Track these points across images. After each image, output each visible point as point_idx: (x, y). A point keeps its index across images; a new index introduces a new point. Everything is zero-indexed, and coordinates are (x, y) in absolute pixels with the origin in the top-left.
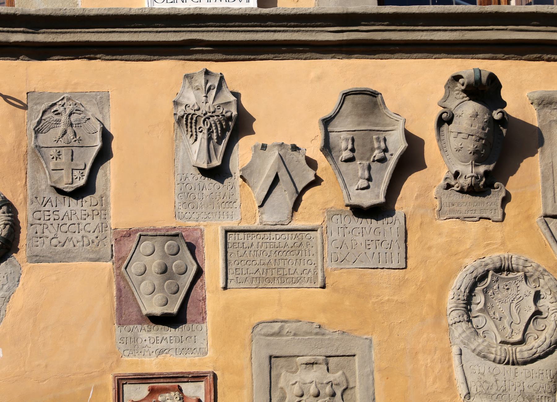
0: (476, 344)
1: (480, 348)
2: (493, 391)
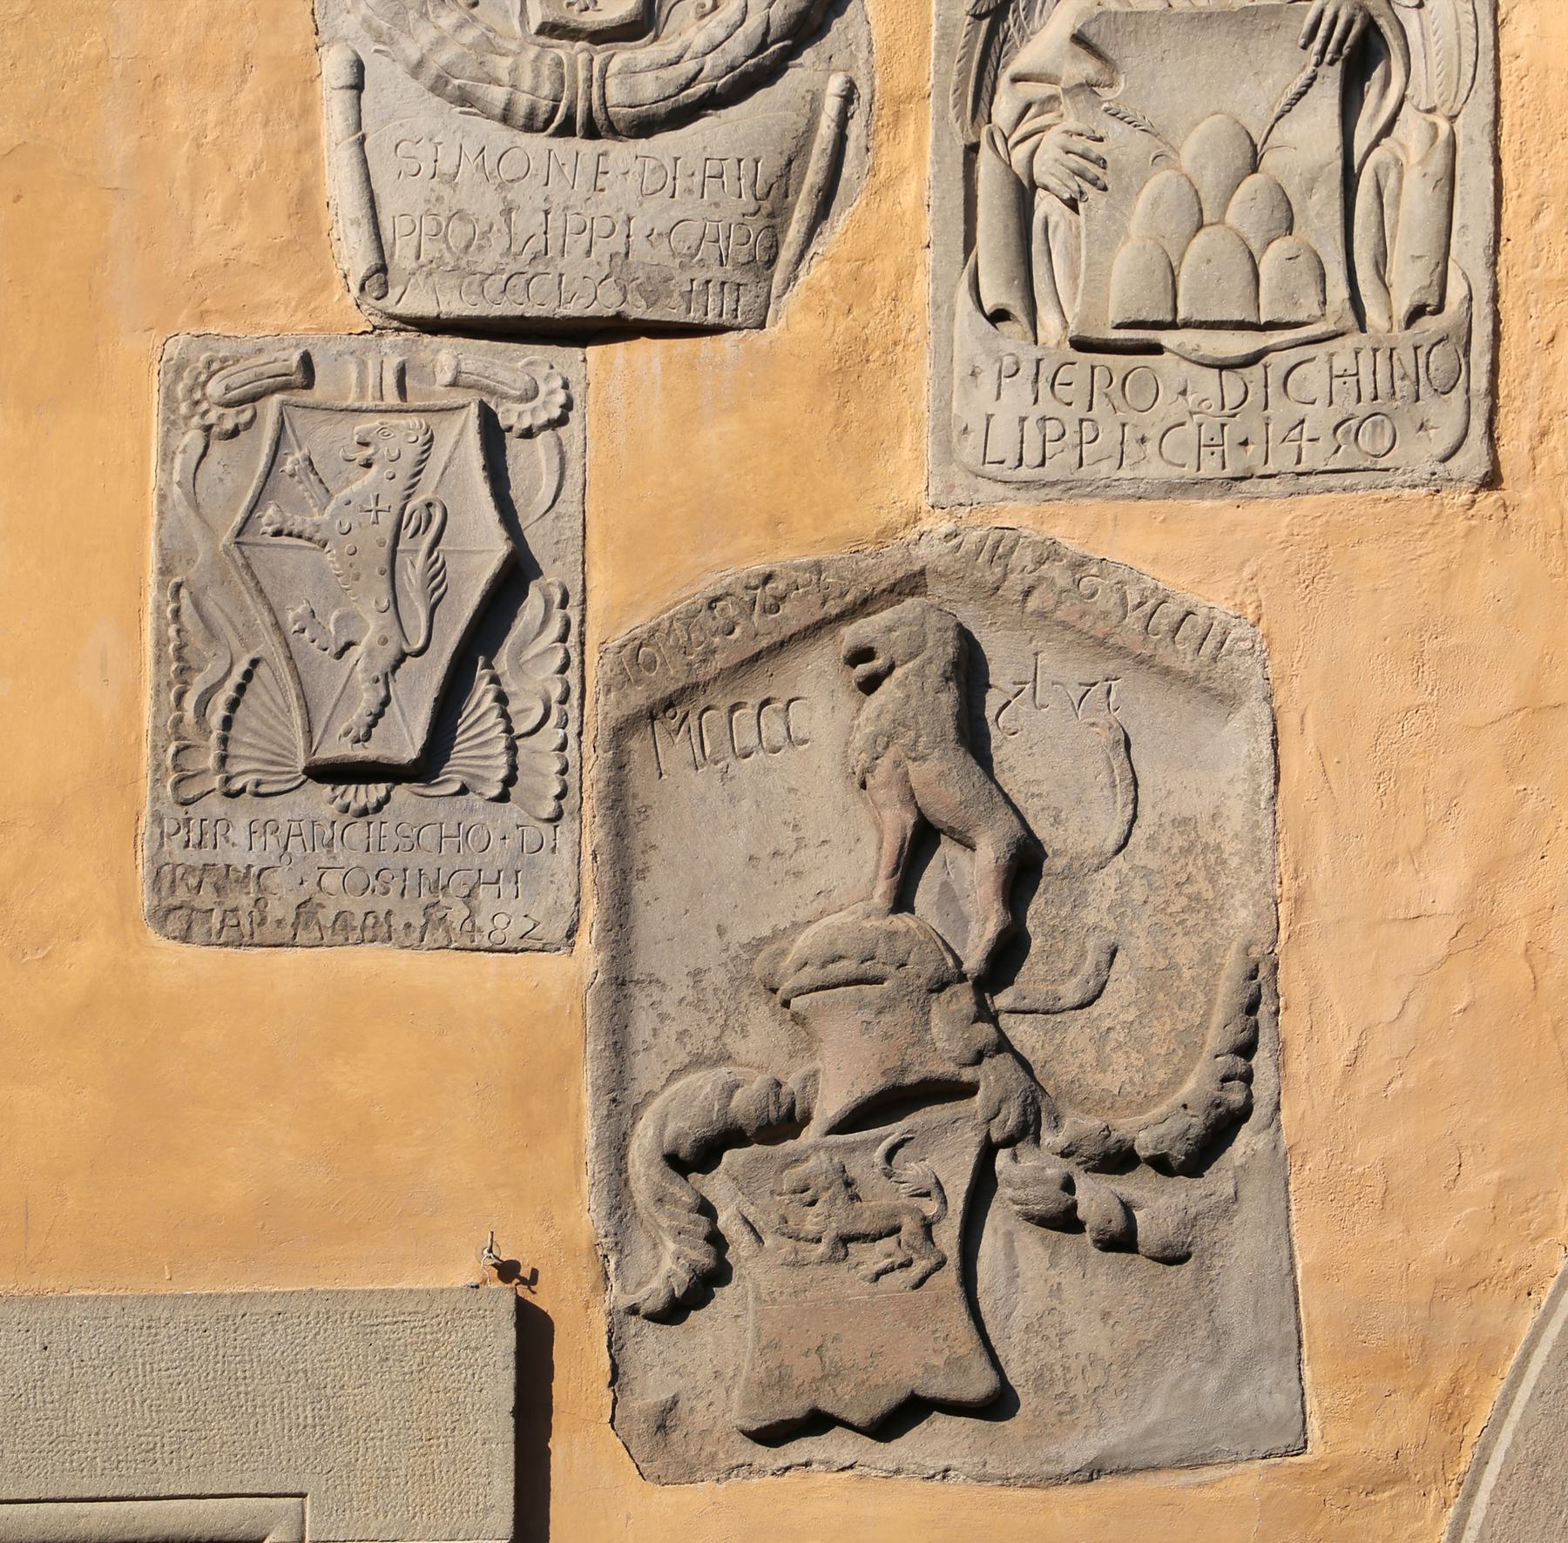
0: (426, 35)
1: (444, 57)
2: (489, 259)
